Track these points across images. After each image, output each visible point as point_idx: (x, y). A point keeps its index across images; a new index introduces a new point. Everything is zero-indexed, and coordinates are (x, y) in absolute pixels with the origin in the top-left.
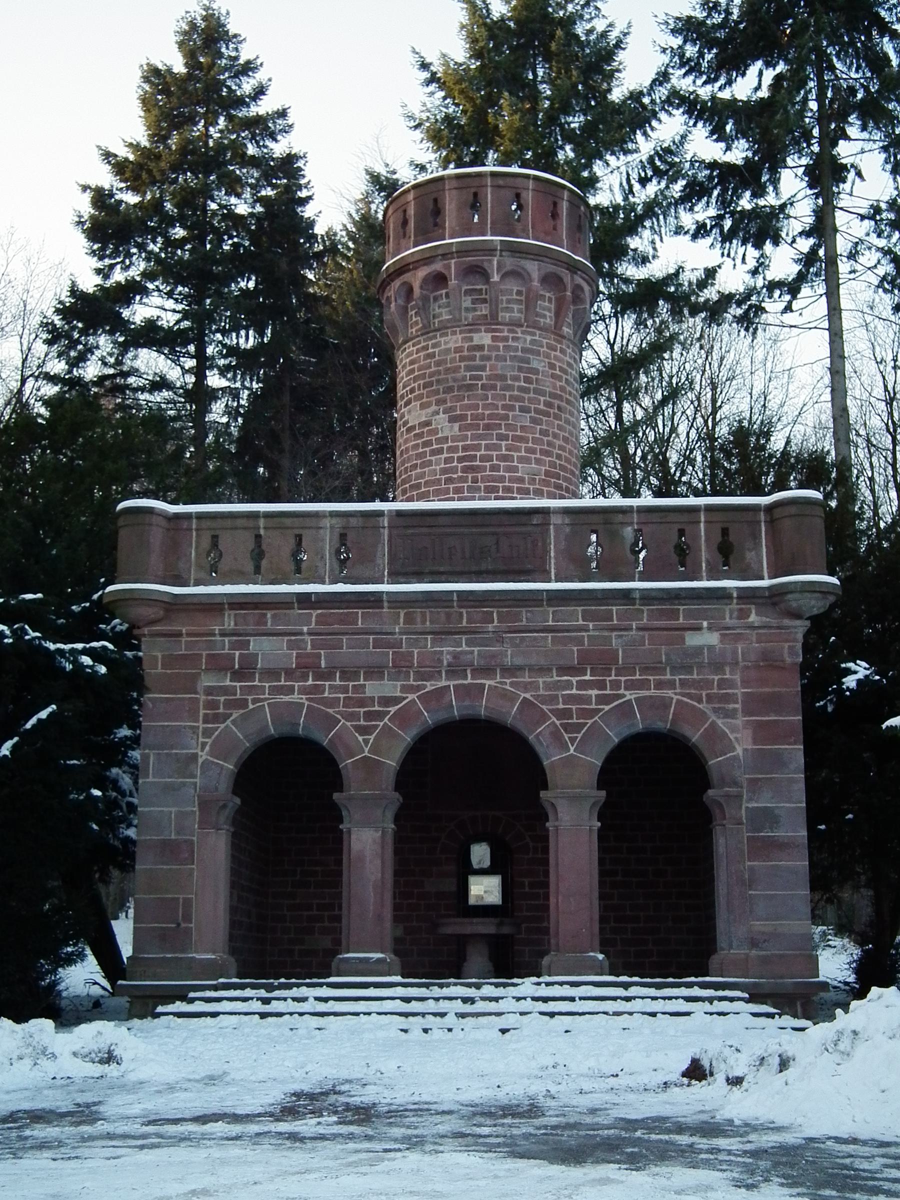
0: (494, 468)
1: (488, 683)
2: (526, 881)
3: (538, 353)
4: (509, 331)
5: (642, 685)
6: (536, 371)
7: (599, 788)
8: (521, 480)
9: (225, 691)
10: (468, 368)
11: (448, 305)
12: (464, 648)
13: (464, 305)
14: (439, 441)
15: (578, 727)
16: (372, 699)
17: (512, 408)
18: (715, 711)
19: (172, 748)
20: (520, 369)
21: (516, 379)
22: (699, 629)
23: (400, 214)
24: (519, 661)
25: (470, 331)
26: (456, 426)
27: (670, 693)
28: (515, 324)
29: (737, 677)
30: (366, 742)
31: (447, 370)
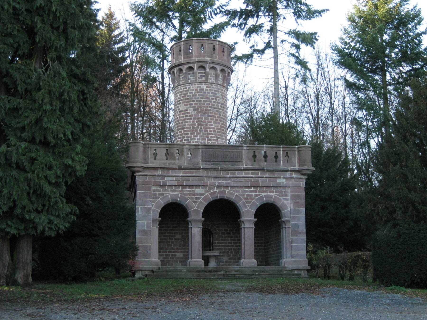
0: (207, 125)
1: (227, 190)
2: (217, 242)
3: (219, 92)
4: (211, 85)
5: (266, 192)
6: (218, 97)
7: (255, 218)
8: (214, 128)
9: (158, 191)
10: (199, 95)
11: (193, 76)
12: (221, 181)
13: (198, 77)
14: (190, 116)
15: (250, 202)
16: (197, 194)
17: (211, 107)
18: (284, 199)
19: (145, 205)
20: (214, 96)
21: (213, 99)
22: (280, 178)
23: (178, 48)
24: (235, 185)
25: (200, 84)
26: (196, 112)
27: (272, 194)
28: (213, 83)
29: (289, 190)
30: (196, 205)
31: (193, 96)
